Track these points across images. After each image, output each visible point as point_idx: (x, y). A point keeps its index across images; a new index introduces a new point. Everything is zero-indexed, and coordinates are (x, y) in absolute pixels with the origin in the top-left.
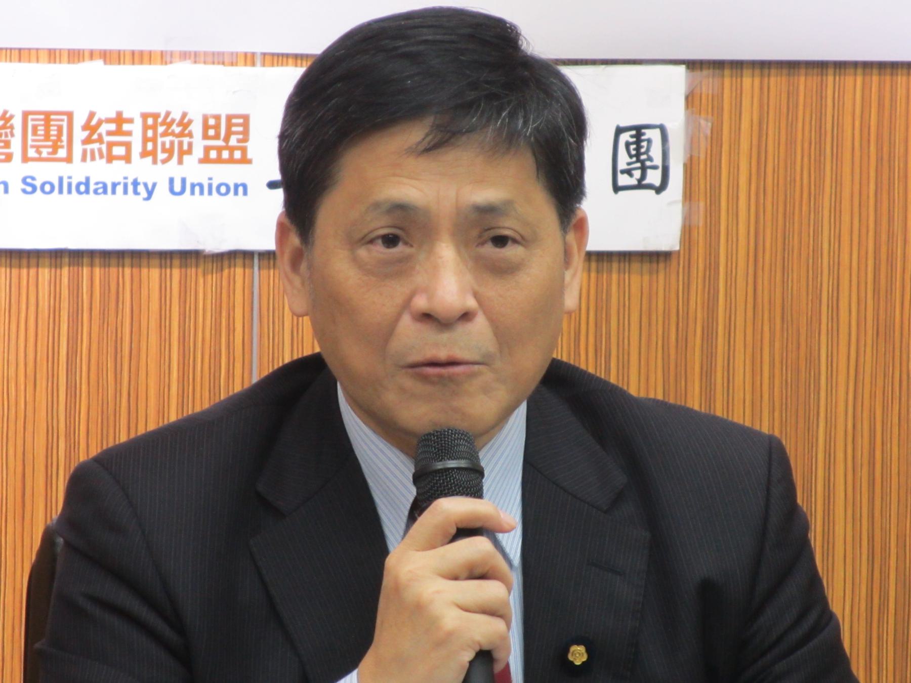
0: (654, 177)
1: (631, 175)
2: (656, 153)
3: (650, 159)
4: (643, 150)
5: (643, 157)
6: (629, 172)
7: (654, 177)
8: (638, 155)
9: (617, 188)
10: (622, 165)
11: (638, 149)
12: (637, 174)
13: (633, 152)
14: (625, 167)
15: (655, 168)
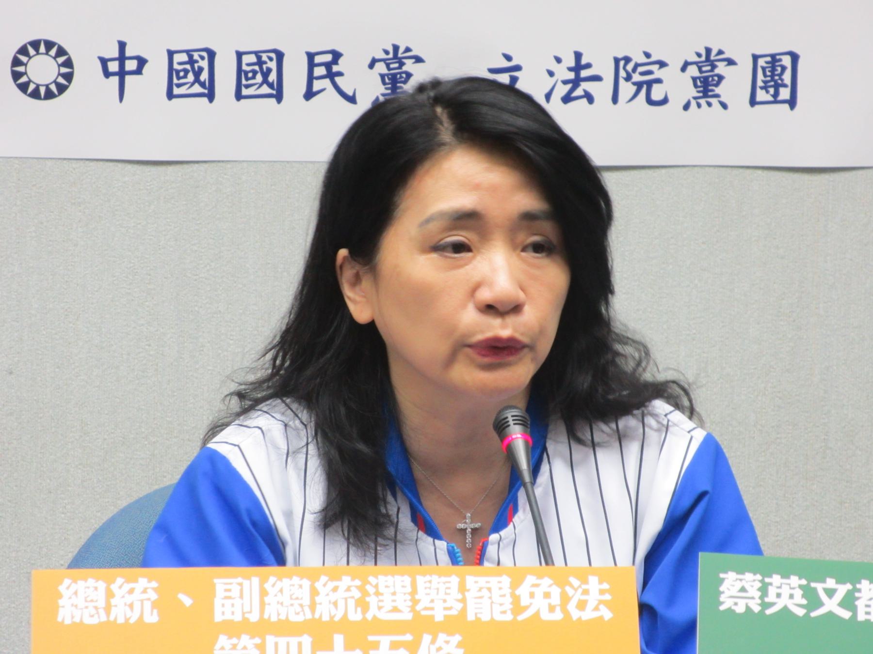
0: (785, 94)
1: (767, 92)
2: (787, 78)
3: (782, 80)
4: (776, 73)
5: (777, 78)
6: (765, 88)
7: (785, 94)
8: (772, 76)
9: (753, 102)
10: (760, 83)
11: (773, 70)
12: (772, 91)
13: (769, 74)
14: (762, 84)
15: (785, 86)
